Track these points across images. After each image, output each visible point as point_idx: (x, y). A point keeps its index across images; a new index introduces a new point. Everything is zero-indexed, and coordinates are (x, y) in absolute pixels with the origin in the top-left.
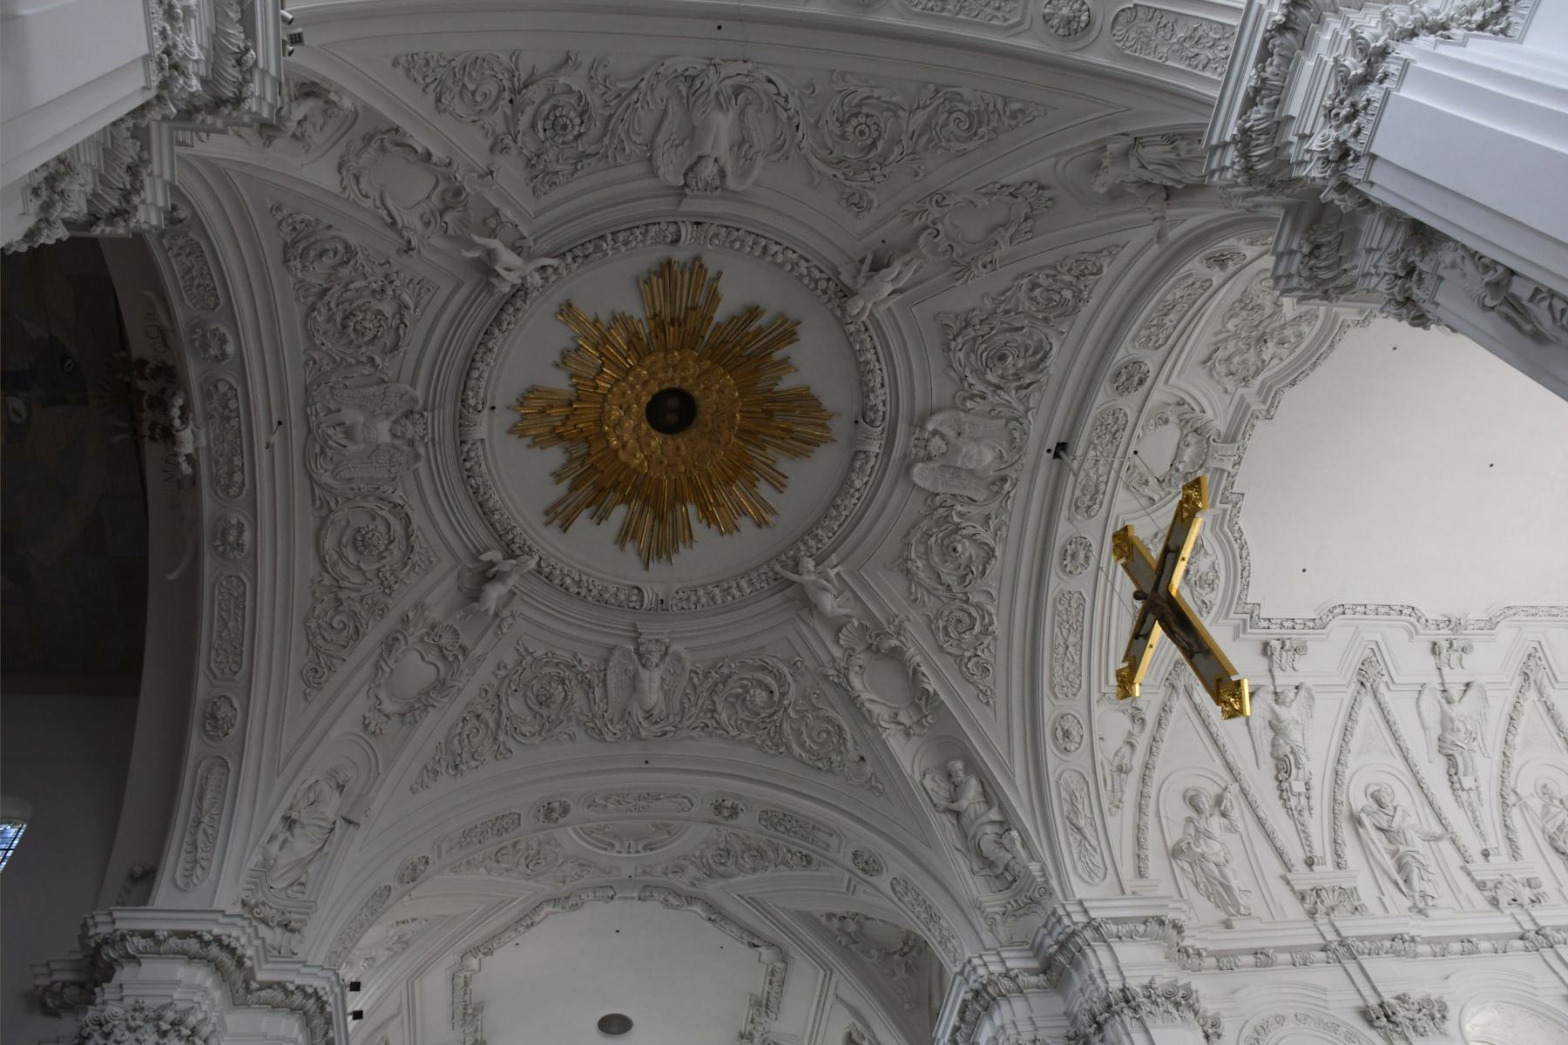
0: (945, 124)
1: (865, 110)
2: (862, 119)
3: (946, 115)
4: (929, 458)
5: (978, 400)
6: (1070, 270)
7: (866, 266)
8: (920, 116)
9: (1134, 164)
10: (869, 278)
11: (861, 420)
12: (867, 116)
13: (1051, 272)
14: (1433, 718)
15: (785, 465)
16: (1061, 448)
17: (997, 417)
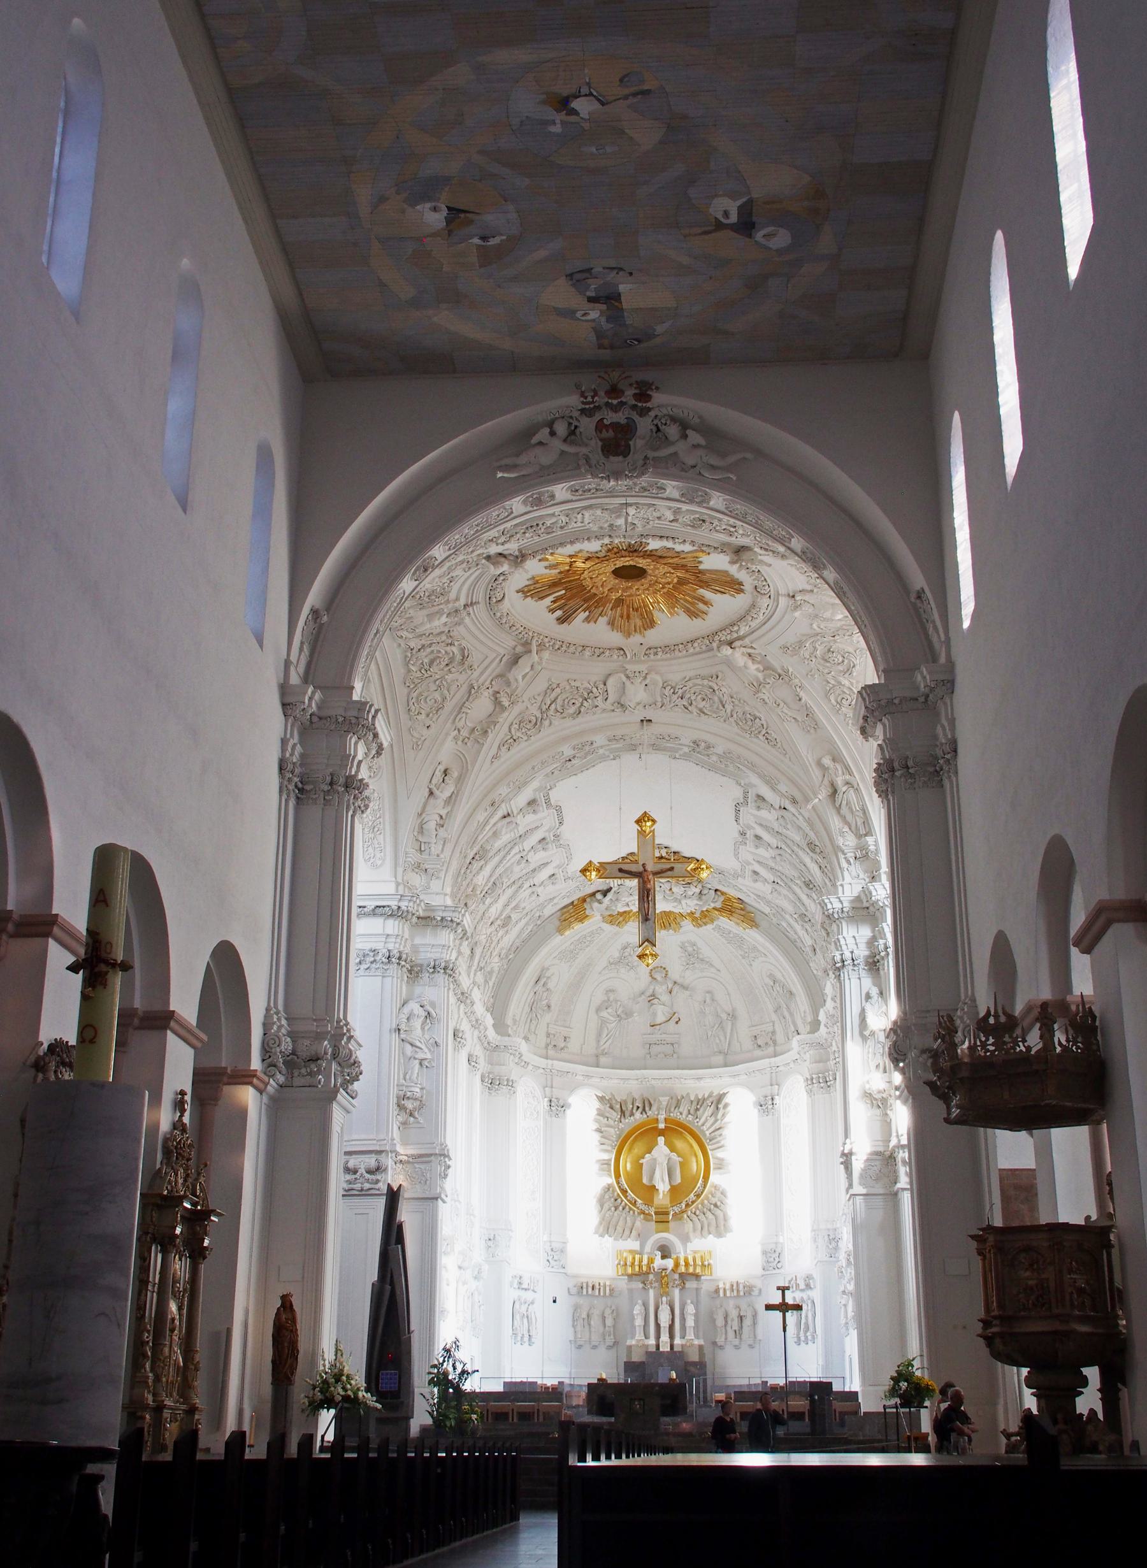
0: (844, 692)
1: (846, 661)
2: (841, 659)
3: (848, 693)
4: (628, 677)
5: (672, 691)
6: (767, 733)
7: (750, 651)
8: (846, 683)
9: (844, 789)
10: (743, 654)
11: (644, 648)
12: (843, 661)
13: (765, 726)
14: (509, 864)
15: (603, 620)
16: (650, 721)
17: (662, 697)
